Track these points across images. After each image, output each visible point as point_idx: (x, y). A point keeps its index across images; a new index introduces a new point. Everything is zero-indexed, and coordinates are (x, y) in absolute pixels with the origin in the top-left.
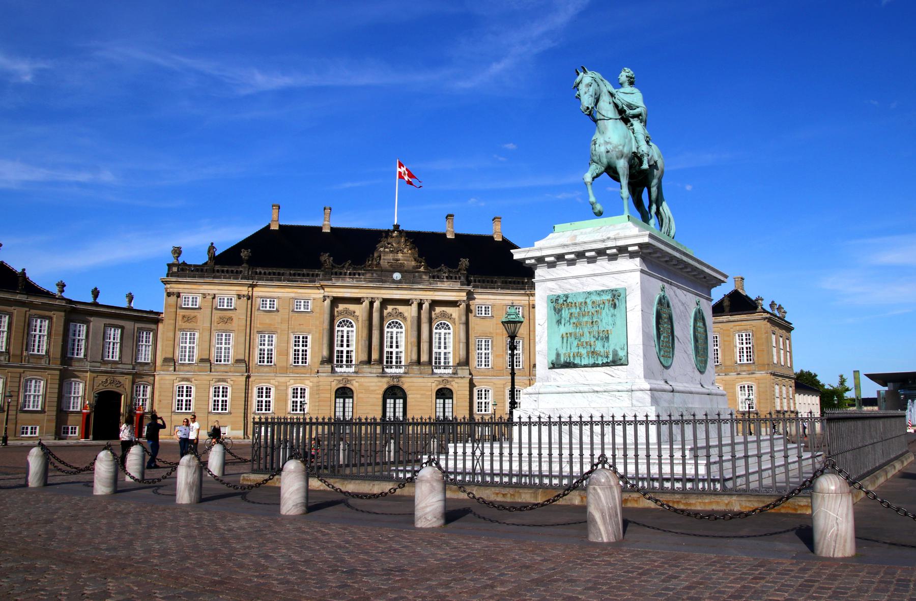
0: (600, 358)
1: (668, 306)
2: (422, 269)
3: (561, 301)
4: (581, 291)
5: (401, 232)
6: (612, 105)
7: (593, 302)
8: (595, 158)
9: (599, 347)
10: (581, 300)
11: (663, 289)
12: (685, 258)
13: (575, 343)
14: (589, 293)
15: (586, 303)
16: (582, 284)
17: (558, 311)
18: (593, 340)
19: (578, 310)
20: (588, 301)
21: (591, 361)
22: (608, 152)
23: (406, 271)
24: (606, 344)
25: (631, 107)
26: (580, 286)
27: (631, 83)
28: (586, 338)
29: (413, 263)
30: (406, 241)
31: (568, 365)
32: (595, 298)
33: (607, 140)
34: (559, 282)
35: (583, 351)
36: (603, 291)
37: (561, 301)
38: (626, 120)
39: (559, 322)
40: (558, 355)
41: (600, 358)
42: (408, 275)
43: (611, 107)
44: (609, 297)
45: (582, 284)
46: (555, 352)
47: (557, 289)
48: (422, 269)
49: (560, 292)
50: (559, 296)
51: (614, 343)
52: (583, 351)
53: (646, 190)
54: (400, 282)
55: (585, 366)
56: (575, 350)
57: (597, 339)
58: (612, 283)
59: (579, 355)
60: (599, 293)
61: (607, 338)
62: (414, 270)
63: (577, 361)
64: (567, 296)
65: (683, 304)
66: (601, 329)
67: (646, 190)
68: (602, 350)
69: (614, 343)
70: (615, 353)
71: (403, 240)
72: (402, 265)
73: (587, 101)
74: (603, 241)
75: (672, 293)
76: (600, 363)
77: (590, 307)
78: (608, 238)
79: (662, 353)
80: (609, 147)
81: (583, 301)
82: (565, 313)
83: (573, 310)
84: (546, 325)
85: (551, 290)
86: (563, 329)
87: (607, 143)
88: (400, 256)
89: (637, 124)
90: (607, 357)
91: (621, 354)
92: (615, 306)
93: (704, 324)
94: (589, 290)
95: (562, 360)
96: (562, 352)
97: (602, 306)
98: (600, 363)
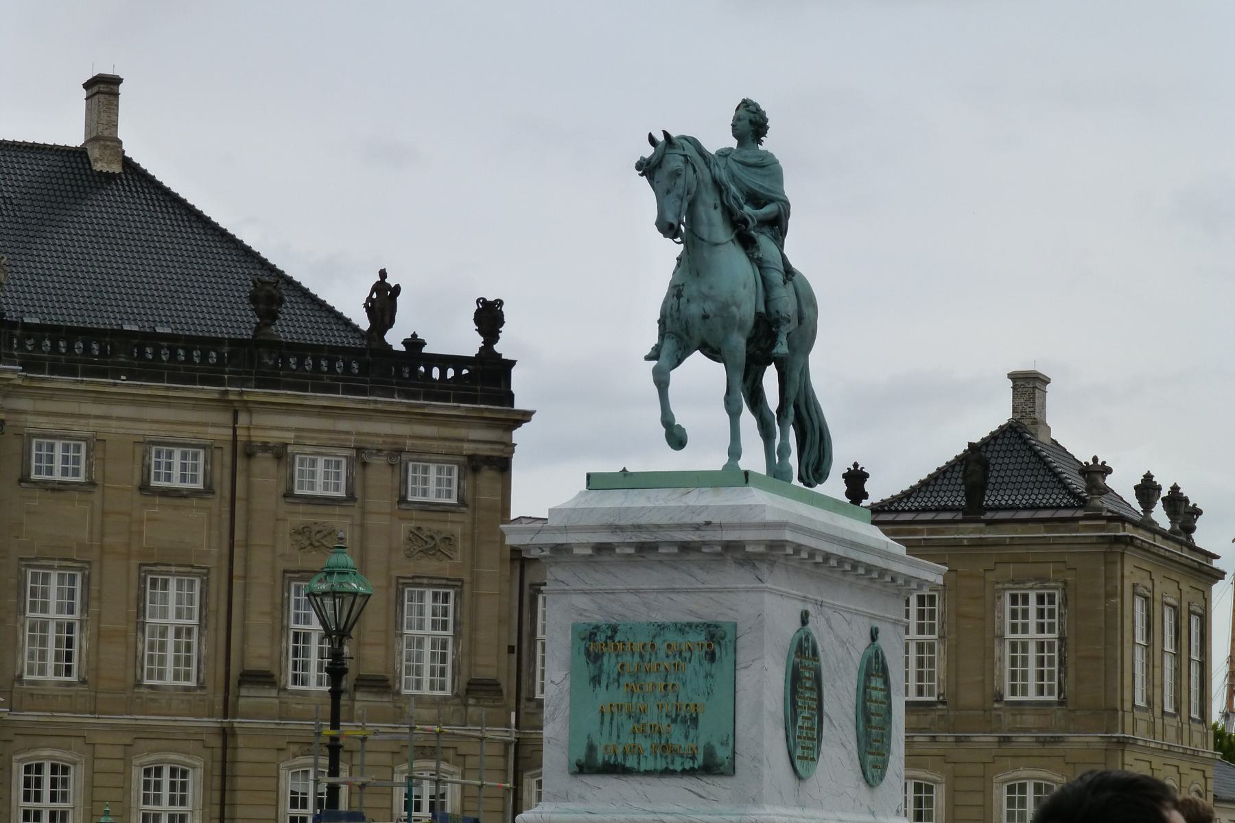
0: (678, 760)
1: (815, 652)
9: (676, 736)
10: (644, 639)
12: (853, 555)
14: (662, 627)
15: (653, 646)
17: (595, 658)
18: (665, 722)
19: (637, 658)
20: (658, 641)
21: (661, 764)
24: (692, 733)
28: (652, 717)
31: (613, 769)
32: (672, 637)
35: (645, 744)
36: (690, 625)
37: (601, 638)
39: (595, 680)
40: (591, 748)
43: (717, 216)
46: (585, 743)
47: (594, 612)
49: (598, 618)
50: (597, 627)
51: (707, 733)
52: (645, 744)
55: (648, 773)
56: (627, 739)
57: (674, 721)
60: (682, 629)
61: (695, 721)
63: (631, 762)
64: (615, 629)
65: (843, 643)
66: (683, 700)
69: (707, 733)
70: (710, 752)
74: (697, 527)
76: (679, 768)
77: (662, 654)
78: (708, 524)
79: (799, 752)
82: (610, 663)
83: (627, 658)
84: (567, 684)
86: (604, 696)
87: (706, 298)
90: (693, 758)
91: (722, 753)
92: (712, 657)
93: (886, 682)
94: (658, 618)
95: (600, 758)
96: (601, 742)
97: (687, 655)
98: (679, 768)
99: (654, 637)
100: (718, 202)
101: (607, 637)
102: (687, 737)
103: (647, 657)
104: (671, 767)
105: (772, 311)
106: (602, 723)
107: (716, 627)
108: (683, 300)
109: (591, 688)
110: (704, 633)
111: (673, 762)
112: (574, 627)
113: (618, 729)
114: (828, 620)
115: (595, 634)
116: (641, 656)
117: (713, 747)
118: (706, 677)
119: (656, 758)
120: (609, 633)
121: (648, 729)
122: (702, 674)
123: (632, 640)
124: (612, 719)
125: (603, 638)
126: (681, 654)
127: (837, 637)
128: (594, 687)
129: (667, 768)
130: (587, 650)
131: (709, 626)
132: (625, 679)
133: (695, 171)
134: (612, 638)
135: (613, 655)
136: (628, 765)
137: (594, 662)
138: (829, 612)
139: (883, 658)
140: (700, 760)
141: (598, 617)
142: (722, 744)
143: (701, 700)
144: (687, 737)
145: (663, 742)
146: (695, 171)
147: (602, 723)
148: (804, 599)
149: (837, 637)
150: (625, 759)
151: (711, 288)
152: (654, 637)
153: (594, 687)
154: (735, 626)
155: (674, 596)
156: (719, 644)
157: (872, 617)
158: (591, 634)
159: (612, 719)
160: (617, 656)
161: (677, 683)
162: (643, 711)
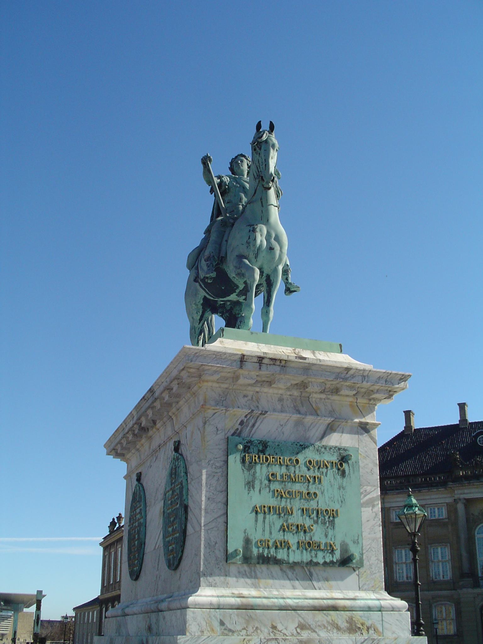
9: (318, 534)
13: (278, 523)
21: (306, 557)
24: (330, 533)
28: (297, 519)
35: (292, 539)
39: (250, 485)
41: (320, 554)
50: (250, 442)
52: (292, 539)
56: (279, 536)
59: (286, 545)
61: (332, 523)
63: (281, 554)
66: (323, 506)
68: (323, 541)
70: (345, 548)
76: (321, 561)
91: (354, 550)
98: (321, 561)
102: (326, 536)
104: (315, 560)
106: (256, 521)
107: (345, 450)
109: (247, 492)
111: (316, 556)
113: (270, 527)
115: (249, 448)
117: (347, 545)
118: (339, 488)
119: (302, 552)
120: (261, 448)
121: (294, 528)
122: (336, 486)
124: (264, 518)
128: (249, 490)
129: (311, 561)
131: (339, 449)
132: (275, 486)
136: (279, 557)
137: (249, 470)
140: (337, 556)
142: (354, 542)
143: (336, 506)
144: (326, 536)
145: (307, 539)
147: (256, 521)
150: (276, 552)
153: (249, 490)
159: (264, 518)
161: (317, 492)
162: (289, 513)
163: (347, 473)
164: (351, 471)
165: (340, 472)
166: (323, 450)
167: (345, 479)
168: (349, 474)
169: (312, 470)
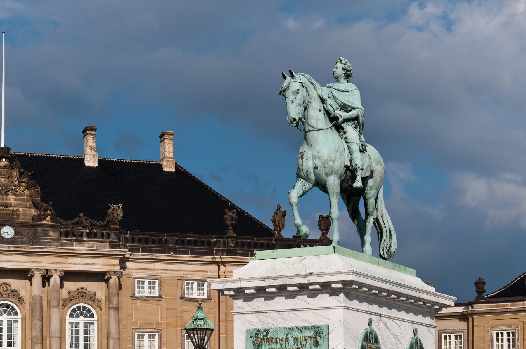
1: (376, 340)
2: (48, 221)
3: (261, 336)
4: (282, 326)
5: (12, 159)
6: (323, 111)
7: (295, 339)
8: (302, 174)
10: (282, 336)
11: (370, 323)
12: (396, 289)
14: (291, 329)
15: (287, 339)
16: (284, 319)
19: (279, 346)
20: (289, 337)
22: (316, 168)
23: (22, 225)
25: (345, 108)
26: (282, 321)
27: (348, 76)
29: (33, 211)
30: (21, 174)
33: (316, 154)
34: (260, 316)
36: (305, 327)
37: (261, 336)
38: (339, 128)
42: (26, 231)
43: (322, 115)
44: (309, 334)
45: (284, 319)
47: (258, 323)
48: (48, 221)
49: (260, 326)
50: (259, 331)
53: (362, 199)
54: (12, 241)
58: (313, 319)
60: (301, 329)
62: (35, 223)
64: (267, 331)
65: (396, 336)
67: (362, 199)
71: (16, 173)
72: (16, 214)
73: (294, 111)
74: (306, 276)
75: (382, 325)
78: (311, 274)
80: (318, 163)
81: (284, 336)
85: (251, 323)
87: (314, 157)
88: (11, 198)
89: (351, 130)
92: (317, 344)
94: (290, 325)
99: (287, 334)
100: (322, 108)
101: (264, 336)
103: (284, 345)
105: (354, 165)
107: (319, 328)
108: (304, 160)
110: (312, 331)
112: (247, 331)
114: (385, 324)
115: (258, 334)
116: (281, 345)
123: (276, 337)
125: (262, 336)
126: (301, 343)
127: (391, 333)
130: (254, 342)
131: (315, 327)
133: (307, 91)
134: (266, 336)
135: (267, 344)
138: (386, 320)
139: (421, 344)
141: (260, 326)
146: (307, 91)
148: (370, 313)
149: (391, 333)
151: (318, 152)
152: (287, 334)
154: (328, 327)
155: (297, 313)
156: (320, 336)
157: (414, 323)
158: (256, 334)
160: (269, 345)
163: (319, 343)
164: (322, 341)
165: (315, 343)
166: (304, 329)
167: (318, 348)
168: (321, 344)
169: (296, 345)
